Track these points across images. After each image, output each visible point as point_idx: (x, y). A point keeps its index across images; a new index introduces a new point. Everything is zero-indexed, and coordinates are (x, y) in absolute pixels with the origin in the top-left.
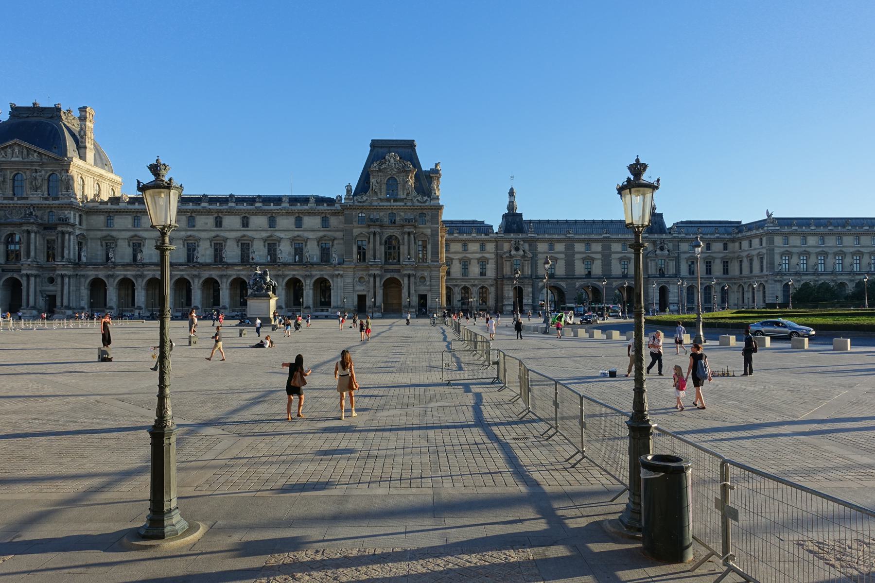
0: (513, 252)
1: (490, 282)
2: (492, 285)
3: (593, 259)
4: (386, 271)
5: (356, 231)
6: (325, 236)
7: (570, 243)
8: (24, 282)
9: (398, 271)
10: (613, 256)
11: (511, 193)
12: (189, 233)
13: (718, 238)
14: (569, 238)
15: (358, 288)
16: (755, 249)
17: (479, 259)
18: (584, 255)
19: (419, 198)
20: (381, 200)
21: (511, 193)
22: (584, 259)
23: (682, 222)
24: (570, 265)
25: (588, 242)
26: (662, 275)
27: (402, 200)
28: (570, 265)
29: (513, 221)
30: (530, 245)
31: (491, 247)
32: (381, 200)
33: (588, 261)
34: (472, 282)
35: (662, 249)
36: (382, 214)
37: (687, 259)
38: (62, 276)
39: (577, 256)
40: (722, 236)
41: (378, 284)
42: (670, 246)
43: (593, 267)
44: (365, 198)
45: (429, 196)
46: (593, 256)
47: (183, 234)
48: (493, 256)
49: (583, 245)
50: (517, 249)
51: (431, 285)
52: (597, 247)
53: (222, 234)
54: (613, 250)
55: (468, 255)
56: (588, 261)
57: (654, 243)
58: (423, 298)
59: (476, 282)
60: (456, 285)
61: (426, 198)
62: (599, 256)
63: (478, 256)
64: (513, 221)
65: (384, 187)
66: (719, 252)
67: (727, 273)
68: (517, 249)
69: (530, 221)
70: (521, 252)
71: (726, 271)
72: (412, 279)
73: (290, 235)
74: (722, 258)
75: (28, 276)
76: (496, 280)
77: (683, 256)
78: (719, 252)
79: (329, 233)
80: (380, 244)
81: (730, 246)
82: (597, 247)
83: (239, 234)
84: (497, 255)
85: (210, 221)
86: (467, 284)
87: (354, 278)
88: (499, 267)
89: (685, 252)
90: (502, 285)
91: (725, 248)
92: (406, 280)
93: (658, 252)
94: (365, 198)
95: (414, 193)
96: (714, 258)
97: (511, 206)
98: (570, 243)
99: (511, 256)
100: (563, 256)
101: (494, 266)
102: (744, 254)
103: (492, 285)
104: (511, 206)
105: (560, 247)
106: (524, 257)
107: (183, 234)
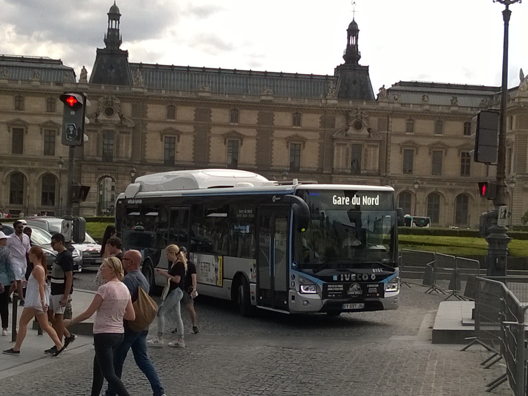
3: (242, 137)
13: (454, 113)
14: (202, 98)
17: (42, 126)
18: (226, 130)
23: (401, 83)
25: (235, 109)
30: (134, 107)
34: (29, 165)
35: (358, 126)
37: (402, 146)
39: (215, 130)
42: (374, 121)
43: (242, 150)
46: (242, 131)
50: (109, 112)
52: (250, 117)
54: (276, 123)
55: (24, 118)
57: (347, 114)
59: (36, 165)
62: (253, 132)
63: (43, 119)
66: (456, 137)
67: (468, 173)
68: (109, 112)
70: (116, 118)
77: (395, 140)
78: (456, 137)
82: (250, 117)
86: (21, 168)
96: (447, 147)
98: (203, 107)
99: (97, 124)
100: (190, 129)
106: (120, 126)
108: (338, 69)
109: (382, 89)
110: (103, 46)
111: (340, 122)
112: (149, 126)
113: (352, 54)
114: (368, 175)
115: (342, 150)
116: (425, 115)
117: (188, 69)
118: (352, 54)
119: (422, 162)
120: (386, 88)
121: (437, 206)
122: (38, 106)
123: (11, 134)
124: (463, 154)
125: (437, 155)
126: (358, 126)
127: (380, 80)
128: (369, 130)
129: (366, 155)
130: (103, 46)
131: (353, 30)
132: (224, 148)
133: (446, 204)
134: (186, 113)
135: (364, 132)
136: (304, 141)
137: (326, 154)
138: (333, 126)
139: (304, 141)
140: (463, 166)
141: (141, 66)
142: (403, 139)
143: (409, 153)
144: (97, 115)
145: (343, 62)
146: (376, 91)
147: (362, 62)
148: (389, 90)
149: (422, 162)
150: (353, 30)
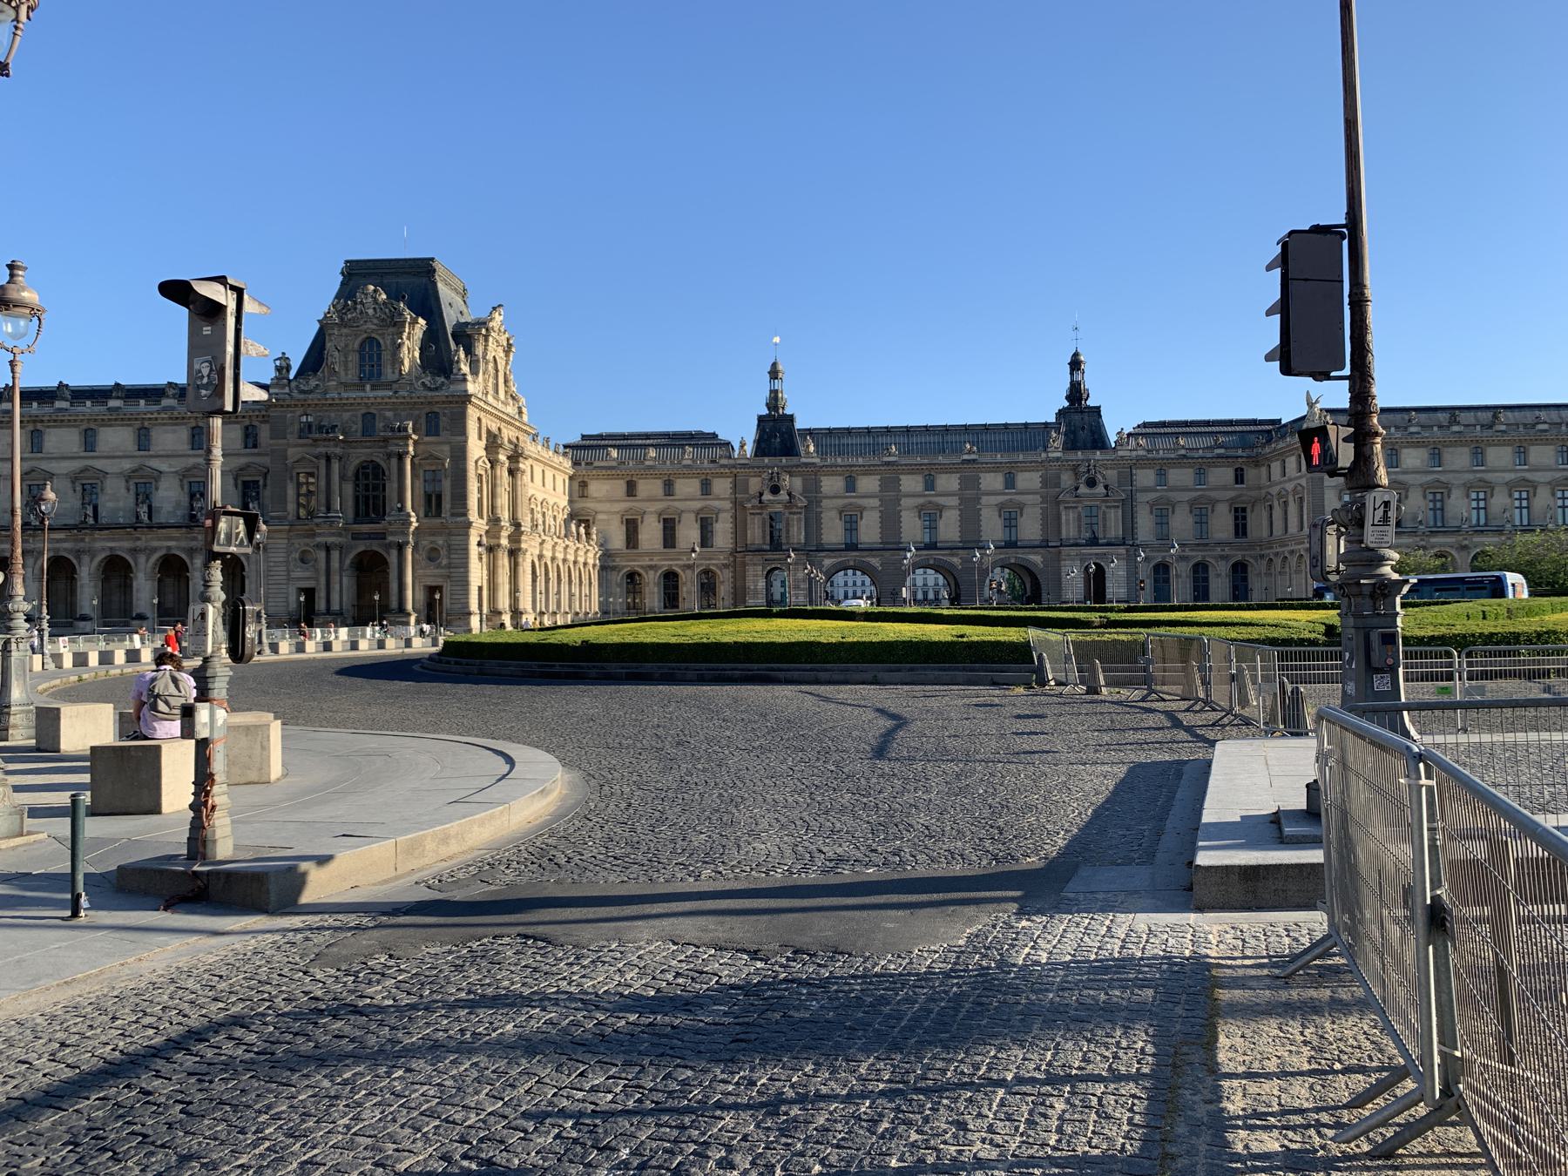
0: (767, 497)
1: (722, 559)
2: (726, 566)
3: (941, 509)
4: (356, 536)
5: (293, 453)
6: (248, 466)
7: (969, 474)
9: (382, 536)
10: (984, 500)
14: (888, 464)
15: (297, 574)
16: (1290, 480)
18: (921, 500)
19: (427, 380)
20: (346, 386)
22: (920, 509)
24: (890, 520)
26: (1094, 541)
27: (388, 386)
28: (890, 520)
29: (777, 432)
31: (722, 486)
32: (346, 386)
33: (930, 515)
35: (1091, 483)
36: (346, 416)
37: (1152, 505)
40: (1231, 453)
41: (335, 564)
43: (941, 524)
44: (313, 383)
45: (448, 378)
46: (941, 500)
48: (728, 505)
49: (920, 478)
51: (449, 566)
52: (948, 483)
53: (98, 464)
56: (930, 515)
60: (651, 567)
62: (954, 501)
63: (698, 505)
64: (777, 432)
65: (354, 358)
66: (1225, 488)
67: (1245, 534)
71: (1241, 529)
73: (179, 464)
74: (1232, 501)
76: (734, 552)
79: (258, 460)
80: (342, 478)
81: (1250, 474)
84: (735, 503)
87: (289, 553)
88: (739, 528)
89: (1146, 490)
90: (744, 564)
91: (1239, 478)
92: (394, 553)
93: (1083, 489)
94: (313, 383)
96: (1214, 503)
97: (774, 401)
100: (875, 502)
101: (729, 526)
102: (1274, 490)
103: (726, 566)
104: (774, 401)
105: (948, 483)
106: (790, 503)
108: (1061, 413)
110: (765, 411)
111: (1067, 479)
112: (825, 503)
113: (1076, 393)
114: (1108, 544)
115: (1072, 515)
116: (1182, 461)
117: (869, 431)
118: (1076, 393)
119: (1182, 523)
120: (1126, 432)
121: (1206, 580)
122: (690, 490)
123: (661, 526)
124: (1236, 510)
125: (1201, 511)
126: (1091, 483)
127: (1116, 423)
128: (1106, 487)
129: (1104, 519)
130: (765, 411)
131: (1075, 364)
132: (919, 523)
133: (1218, 575)
134: (869, 484)
135: (1100, 489)
136: (1021, 507)
137: (1051, 521)
138: (1058, 485)
139: (1021, 507)
140: (1236, 526)
141: (810, 432)
142: (1154, 495)
143: (1162, 513)
144: (761, 494)
145: (1066, 404)
146: (1112, 438)
147: (1091, 403)
148: (1129, 435)
149: (1182, 523)
150: (1075, 364)
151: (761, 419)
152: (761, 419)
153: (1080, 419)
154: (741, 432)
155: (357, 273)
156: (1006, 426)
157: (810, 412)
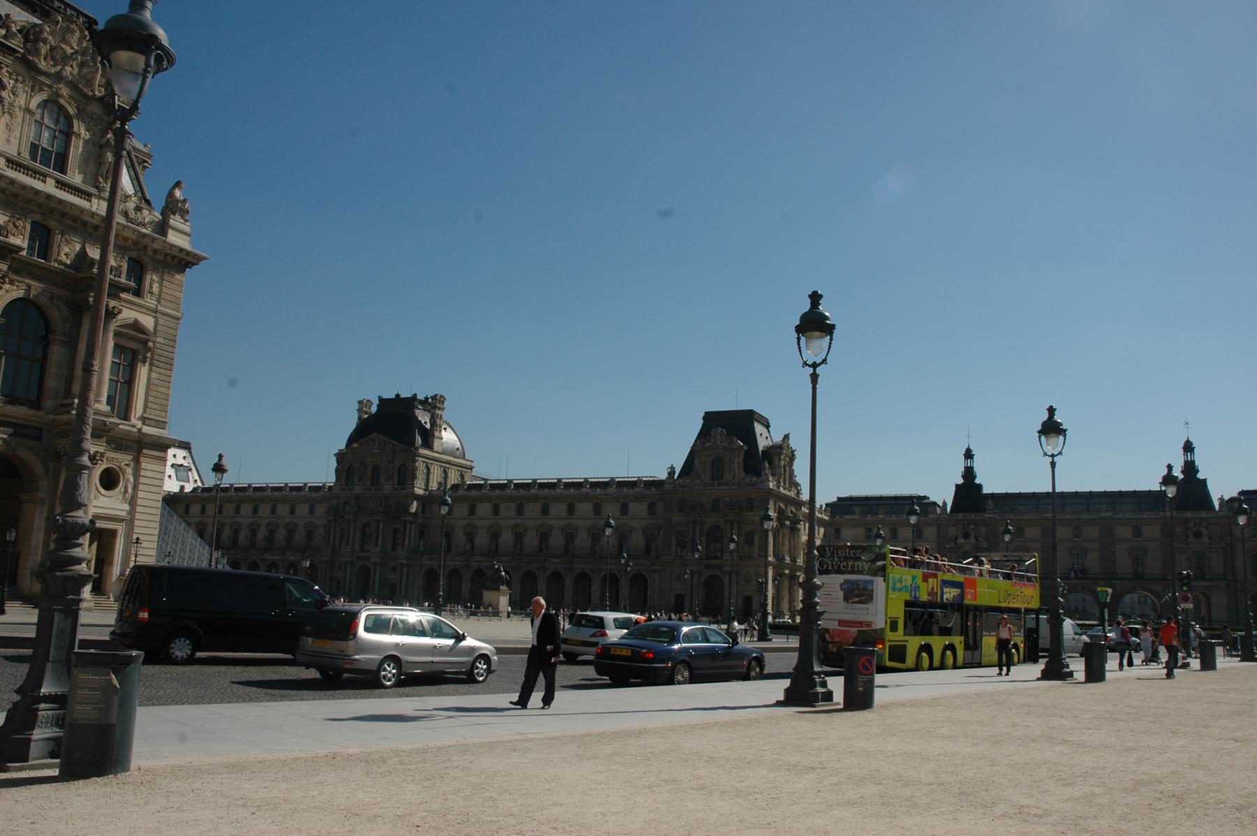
0: (961, 540)
8: (372, 568)
11: (969, 455)
12: (518, 521)
21: (969, 455)
35: (1198, 535)
38: (402, 565)
47: (512, 522)
50: (966, 536)
58: (748, 600)
61: (755, 479)
69: (993, 495)
70: (972, 540)
72: (734, 576)
75: (375, 564)
83: (563, 522)
85: (537, 508)
94: (687, 481)
95: (742, 474)
97: (969, 474)
104: (969, 474)
107: (512, 522)
109: (1221, 499)
110: (961, 481)
126: (1198, 535)
127: (1221, 488)
130: (961, 481)
144: (956, 538)
151: (957, 486)
152: (957, 486)
153: (1189, 486)
154: (943, 493)
155: (712, 420)
156: (1135, 492)
157: (991, 483)
